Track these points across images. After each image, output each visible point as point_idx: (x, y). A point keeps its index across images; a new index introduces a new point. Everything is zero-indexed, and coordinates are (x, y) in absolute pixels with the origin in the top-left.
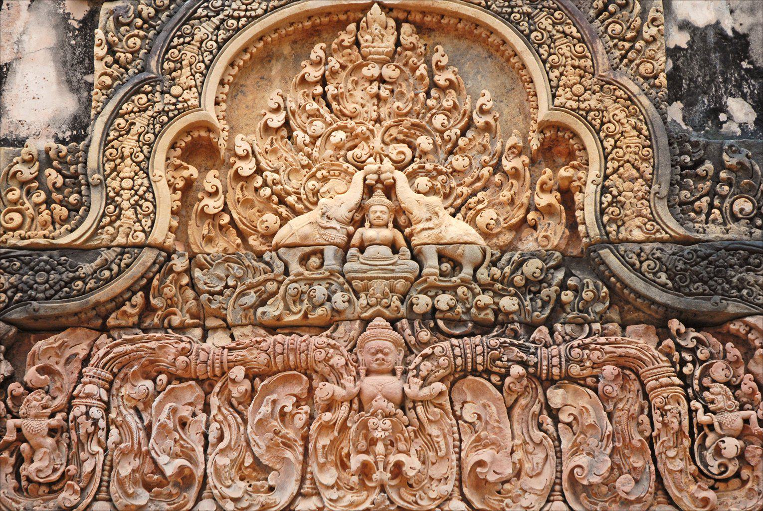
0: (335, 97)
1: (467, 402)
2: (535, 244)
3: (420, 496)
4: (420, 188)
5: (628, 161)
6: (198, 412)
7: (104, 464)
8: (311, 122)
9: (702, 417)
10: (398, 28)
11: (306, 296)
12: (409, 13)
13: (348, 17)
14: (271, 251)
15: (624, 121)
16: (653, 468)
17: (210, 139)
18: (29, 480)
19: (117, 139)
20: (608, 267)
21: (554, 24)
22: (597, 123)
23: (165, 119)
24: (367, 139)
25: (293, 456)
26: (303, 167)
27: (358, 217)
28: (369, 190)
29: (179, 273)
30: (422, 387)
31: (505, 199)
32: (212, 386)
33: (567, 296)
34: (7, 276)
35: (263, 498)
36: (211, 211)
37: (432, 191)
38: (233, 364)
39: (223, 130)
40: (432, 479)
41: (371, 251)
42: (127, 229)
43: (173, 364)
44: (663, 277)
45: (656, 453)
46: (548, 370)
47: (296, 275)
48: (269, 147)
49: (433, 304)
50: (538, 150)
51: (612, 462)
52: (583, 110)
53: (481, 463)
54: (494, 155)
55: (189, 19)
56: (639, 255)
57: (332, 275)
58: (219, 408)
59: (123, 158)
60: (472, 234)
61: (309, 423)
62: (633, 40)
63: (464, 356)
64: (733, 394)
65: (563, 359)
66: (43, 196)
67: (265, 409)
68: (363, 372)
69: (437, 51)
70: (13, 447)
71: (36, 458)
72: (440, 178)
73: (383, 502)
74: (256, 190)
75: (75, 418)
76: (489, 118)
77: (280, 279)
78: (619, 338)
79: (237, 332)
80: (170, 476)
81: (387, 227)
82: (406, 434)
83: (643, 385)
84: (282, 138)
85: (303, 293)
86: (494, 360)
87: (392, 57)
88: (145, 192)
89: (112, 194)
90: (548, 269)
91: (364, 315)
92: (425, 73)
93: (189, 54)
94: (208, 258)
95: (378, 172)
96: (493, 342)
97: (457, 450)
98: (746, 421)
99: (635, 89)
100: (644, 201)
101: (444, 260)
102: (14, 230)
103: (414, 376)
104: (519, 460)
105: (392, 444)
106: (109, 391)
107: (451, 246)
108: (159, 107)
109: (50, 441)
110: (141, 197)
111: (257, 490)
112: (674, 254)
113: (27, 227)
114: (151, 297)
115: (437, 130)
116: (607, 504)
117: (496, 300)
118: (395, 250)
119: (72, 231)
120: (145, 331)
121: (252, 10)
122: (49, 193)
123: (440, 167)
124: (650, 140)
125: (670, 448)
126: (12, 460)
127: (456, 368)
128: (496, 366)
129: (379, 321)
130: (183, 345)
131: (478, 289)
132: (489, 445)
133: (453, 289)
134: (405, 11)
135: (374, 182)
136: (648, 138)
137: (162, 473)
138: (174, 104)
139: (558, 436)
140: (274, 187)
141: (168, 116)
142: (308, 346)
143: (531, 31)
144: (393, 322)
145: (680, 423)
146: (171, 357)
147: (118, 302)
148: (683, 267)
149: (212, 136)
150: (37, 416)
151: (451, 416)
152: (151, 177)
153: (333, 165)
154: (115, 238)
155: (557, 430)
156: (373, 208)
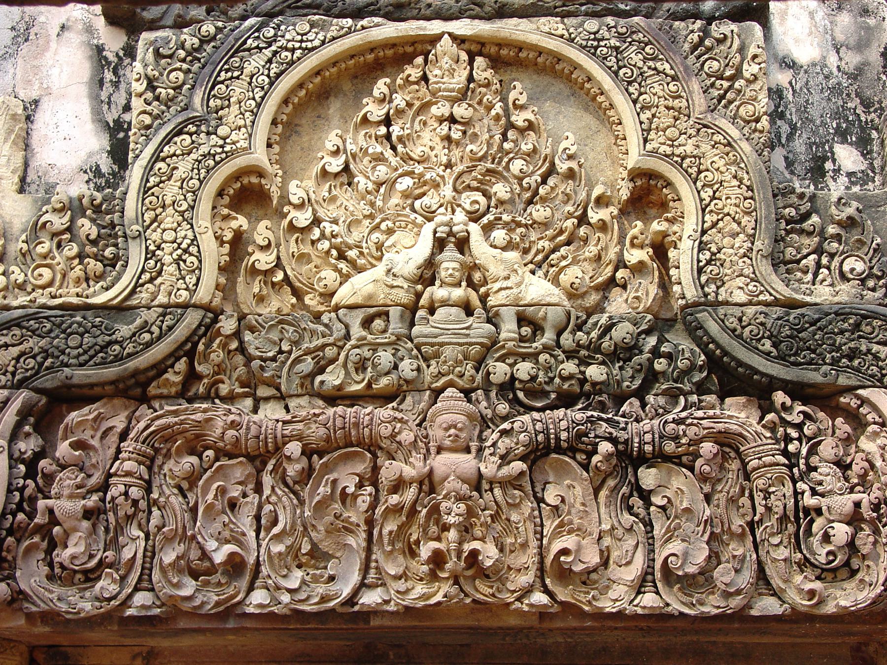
0: (400, 139)
1: (549, 483)
2: (624, 305)
3: (498, 588)
4: (497, 243)
5: (728, 214)
6: (250, 492)
7: (145, 550)
8: (374, 168)
9: (809, 500)
10: (471, 62)
12: (483, 44)
13: (415, 49)
15: (723, 169)
16: (754, 556)
17: (261, 185)
18: (62, 567)
19: (158, 186)
20: (706, 333)
21: (645, 60)
22: (693, 171)
23: (211, 163)
24: (437, 186)
25: (357, 541)
26: (365, 217)
27: (428, 274)
28: (440, 244)
29: (227, 337)
30: (500, 467)
31: (591, 255)
32: (264, 464)
33: (660, 365)
34: (36, 339)
35: (321, 589)
36: (262, 266)
37: (509, 246)
38: (287, 439)
39: (276, 176)
40: (510, 568)
41: (441, 313)
42: (169, 288)
43: (222, 438)
44: (767, 345)
45: (758, 540)
46: (639, 447)
47: (358, 340)
48: (327, 194)
49: (512, 374)
50: (628, 201)
51: (710, 549)
52: (678, 156)
53: (565, 552)
54: (579, 205)
55: (237, 51)
56: (740, 320)
57: (398, 339)
58: (273, 488)
59: (164, 207)
61: (373, 507)
62: (732, 79)
63: (546, 431)
64: (843, 474)
65: (657, 436)
66: (75, 249)
67: (323, 490)
68: (433, 450)
69: (515, 87)
70: (45, 531)
71: (70, 543)
73: (458, 595)
74: (313, 242)
75: (113, 499)
76: (573, 164)
78: (718, 412)
79: (292, 403)
80: (219, 564)
82: (482, 519)
83: (744, 464)
84: (342, 184)
85: (365, 359)
86: (580, 435)
87: (463, 95)
88: (189, 246)
89: (152, 248)
90: (639, 334)
91: (434, 385)
92: (501, 112)
93: (238, 89)
94: (260, 319)
96: (579, 416)
97: (538, 536)
98: (857, 505)
99: (734, 133)
100: (745, 259)
101: (523, 323)
102: (43, 287)
103: (491, 454)
104: (608, 547)
105: (467, 530)
106: (150, 468)
107: (532, 308)
108: (204, 149)
109: (86, 524)
110: (185, 251)
111: (316, 579)
112: (779, 319)
113: (57, 284)
114: (196, 363)
115: (515, 177)
116: (704, 595)
117: (582, 369)
118: (469, 311)
119: (107, 289)
120: (190, 401)
121: (308, 41)
122: (82, 246)
124: (752, 191)
125: (772, 535)
126: (45, 544)
127: (538, 445)
128: (583, 443)
129: (450, 392)
130: (232, 417)
131: (562, 357)
132: (575, 531)
134: (478, 43)
136: (750, 188)
137: (210, 560)
138: (222, 147)
139: (650, 520)
140: (333, 240)
141: (214, 160)
142: (372, 419)
143: (620, 68)
144: (467, 393)
145: (785, 507)
146: (219, 431)
147: (160, 368)
148: (788, 333)
149: (263, 182)
150: (71, 497)
151: (532, 499)
152: (196, 229)
153: (399, 215)
154: (156, 298)
155: (649, 514)
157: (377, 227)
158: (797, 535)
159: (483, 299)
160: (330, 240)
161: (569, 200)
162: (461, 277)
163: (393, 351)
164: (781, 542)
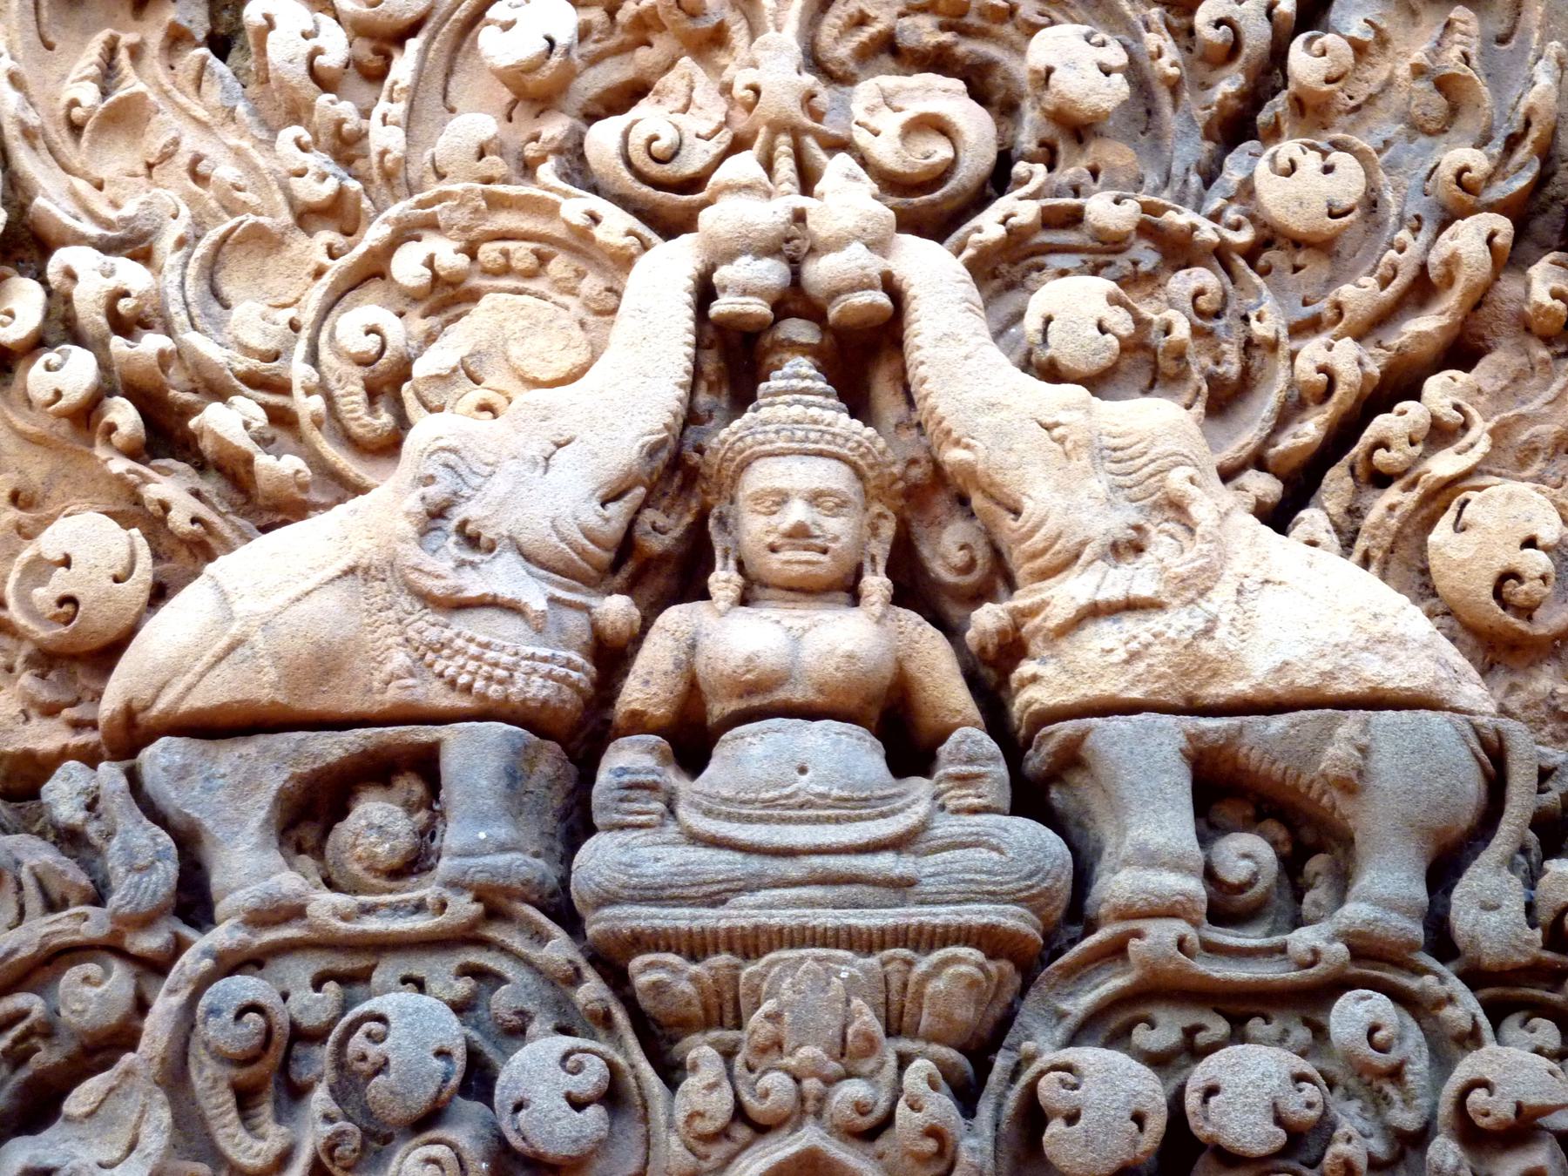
4: (1062, 348)
11: (324, 1054)
14: (90, 758)
26: (308, 216)
27: (664, 532)
28: (732, 357)
37: (1141, 364)
41: (751, 756)
48: (88, 95)
54: (1513, 142)
57: (494, 913)
60: (1416, 650)
72: (1184, 282)
77: (149, 942)
81: (854, 595)
84: (177, 39)
85: (302, 1036)
95: (792, 246)
101: (1225, 812)
107: (1278, 723)
118: (905, 735)
123: (1180, 218)
131: (1465, 1007)
133: (1310, 999)
135: (759, 307)
140: (118, 344)
153: (496, 203)
156: (763, 476)
157: (373, 271)
159: (991, 672)
160: (97, 346)
161: (1454, 111)
162: (861, 546)
163: (463, 987)
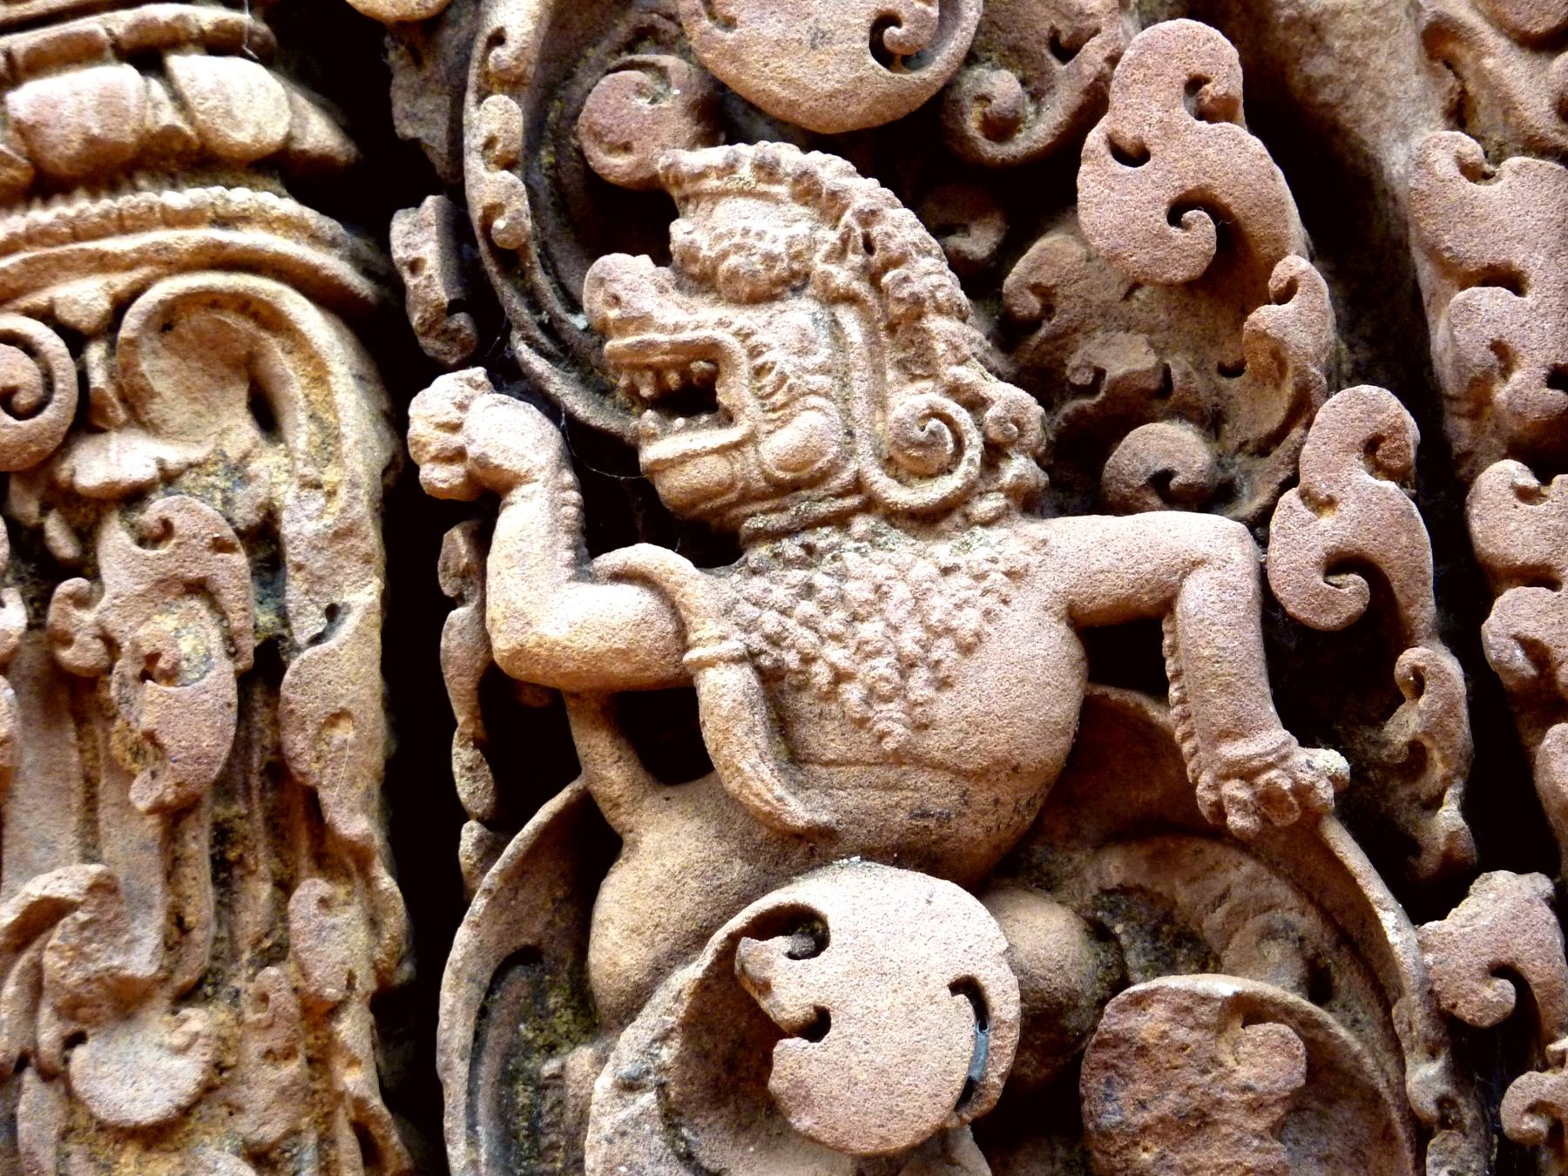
9: (545, 599)
98: (1122, 643)
125: (124, 1002)
145: (263, 670)
158: (404, 1013)
164: (217, 1086)
